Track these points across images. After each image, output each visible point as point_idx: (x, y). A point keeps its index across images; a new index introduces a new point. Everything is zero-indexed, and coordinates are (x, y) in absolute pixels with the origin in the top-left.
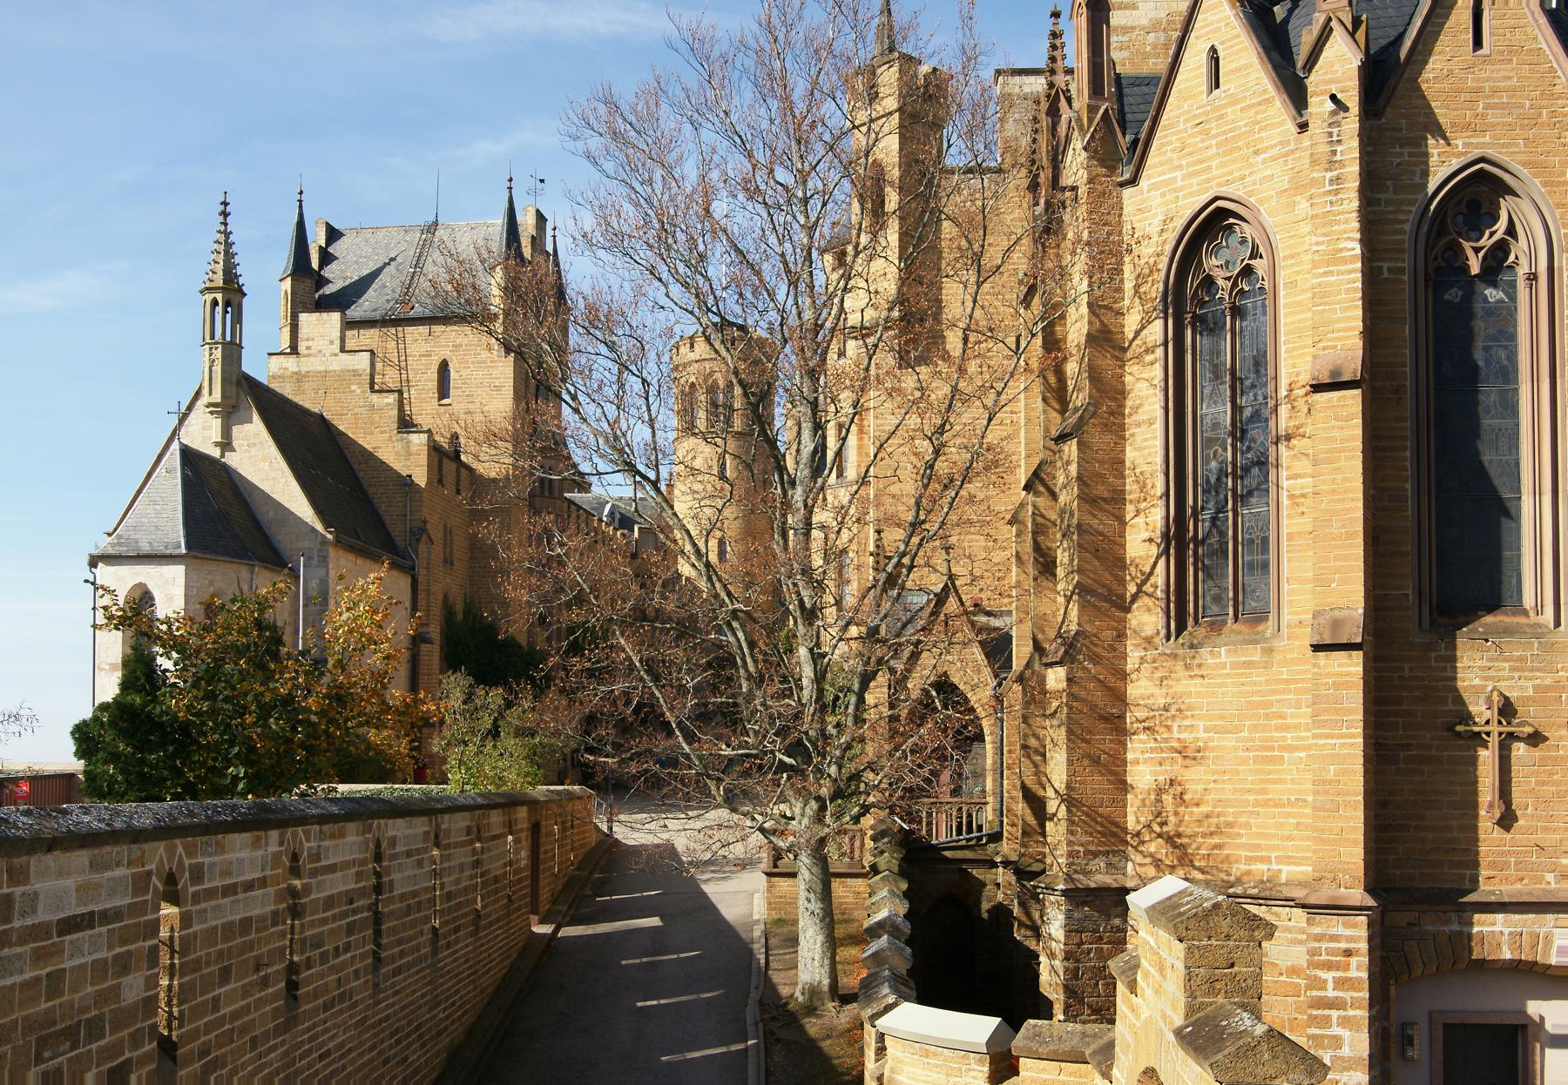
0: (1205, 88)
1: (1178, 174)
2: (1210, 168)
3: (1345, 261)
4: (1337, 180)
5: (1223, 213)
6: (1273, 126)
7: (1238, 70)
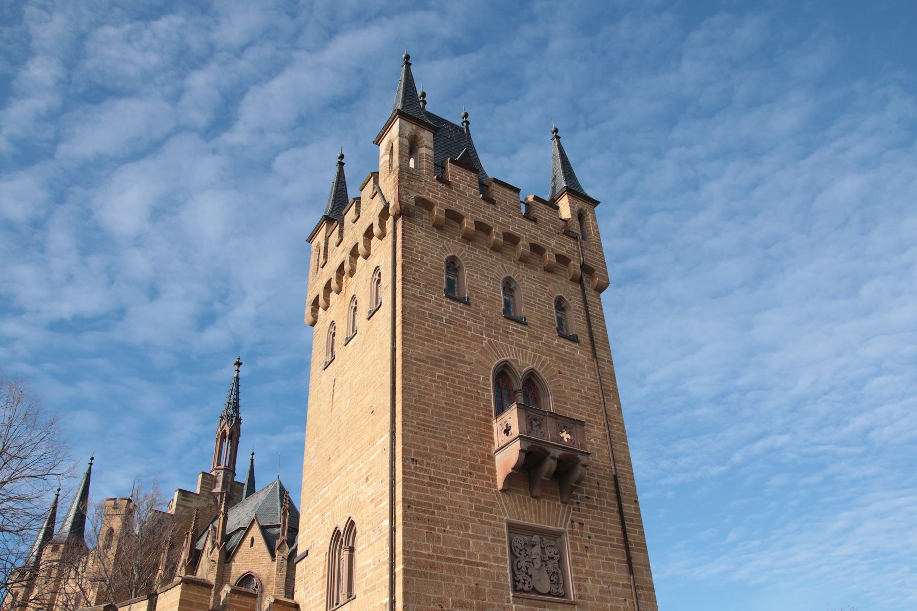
0: (250, 545)
1: (241, 564)
2: (248, 564)
3: (281, 593)
4: (282, 575)
5: (250, 575)
6: (266, 559)
7: (259, 544)
